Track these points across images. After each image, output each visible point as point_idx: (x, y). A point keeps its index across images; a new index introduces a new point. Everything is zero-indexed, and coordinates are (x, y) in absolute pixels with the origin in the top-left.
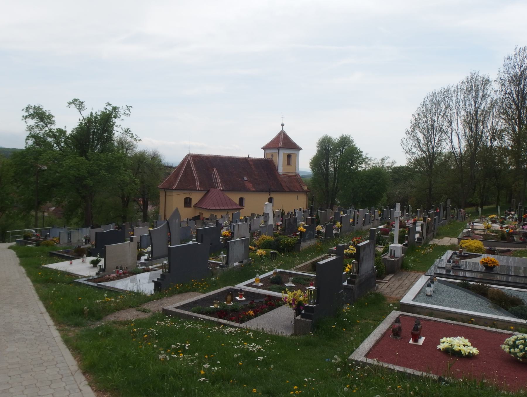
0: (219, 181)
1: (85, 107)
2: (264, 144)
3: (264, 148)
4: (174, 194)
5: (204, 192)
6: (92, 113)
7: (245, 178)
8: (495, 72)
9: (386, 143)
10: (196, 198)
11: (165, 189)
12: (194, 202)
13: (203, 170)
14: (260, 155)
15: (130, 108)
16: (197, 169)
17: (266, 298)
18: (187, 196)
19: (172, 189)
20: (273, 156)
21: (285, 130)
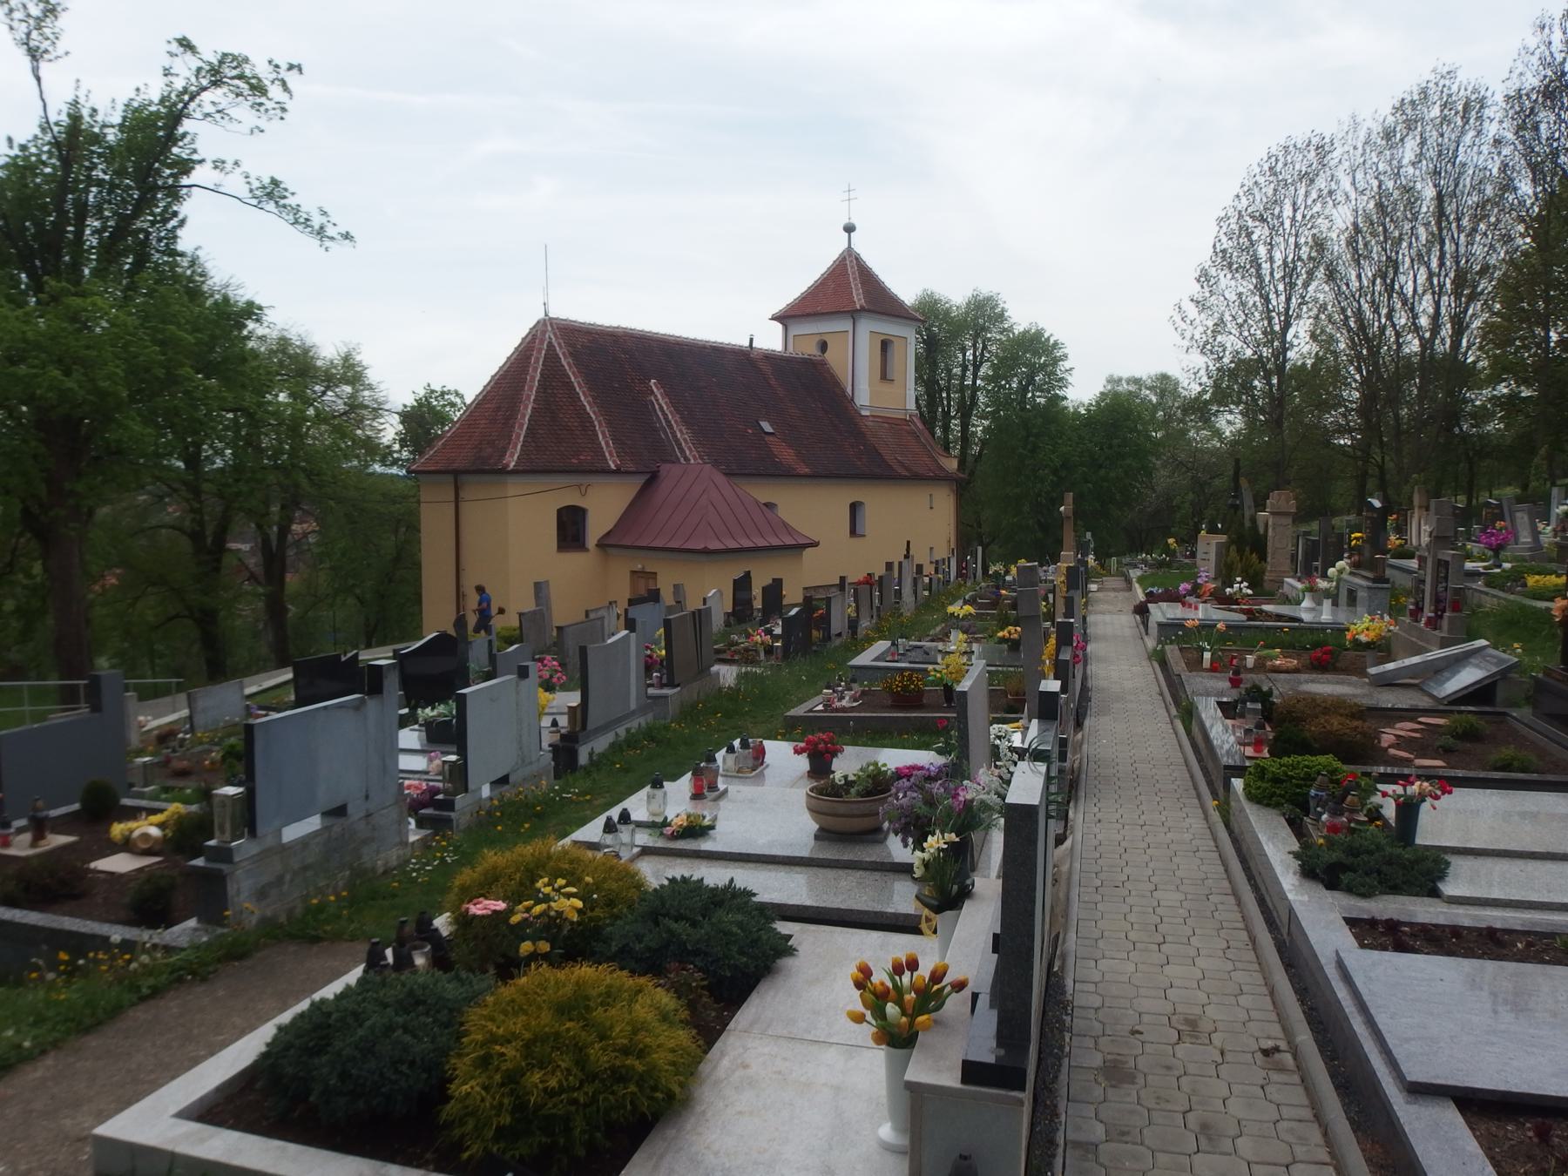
0: (682, 434)
1: (62, 46)
2: (780, 305)
3: (783, 318)
4: (511, 491)
5: (639, 481)
6: (75, 103)
7: (767, 427)
8: (1495, 61)
9: (1127, 313)
10: (605, 505)
11: (456, 473)
12: (597, 527)
13: (591, 396)
14: (771, 339)
15: (292, 79)
16: (592, 383)
17: (1345, 878)
18: (571, 499)
19: (504, 471)
20: (824, 346)
21: (858, 247)
